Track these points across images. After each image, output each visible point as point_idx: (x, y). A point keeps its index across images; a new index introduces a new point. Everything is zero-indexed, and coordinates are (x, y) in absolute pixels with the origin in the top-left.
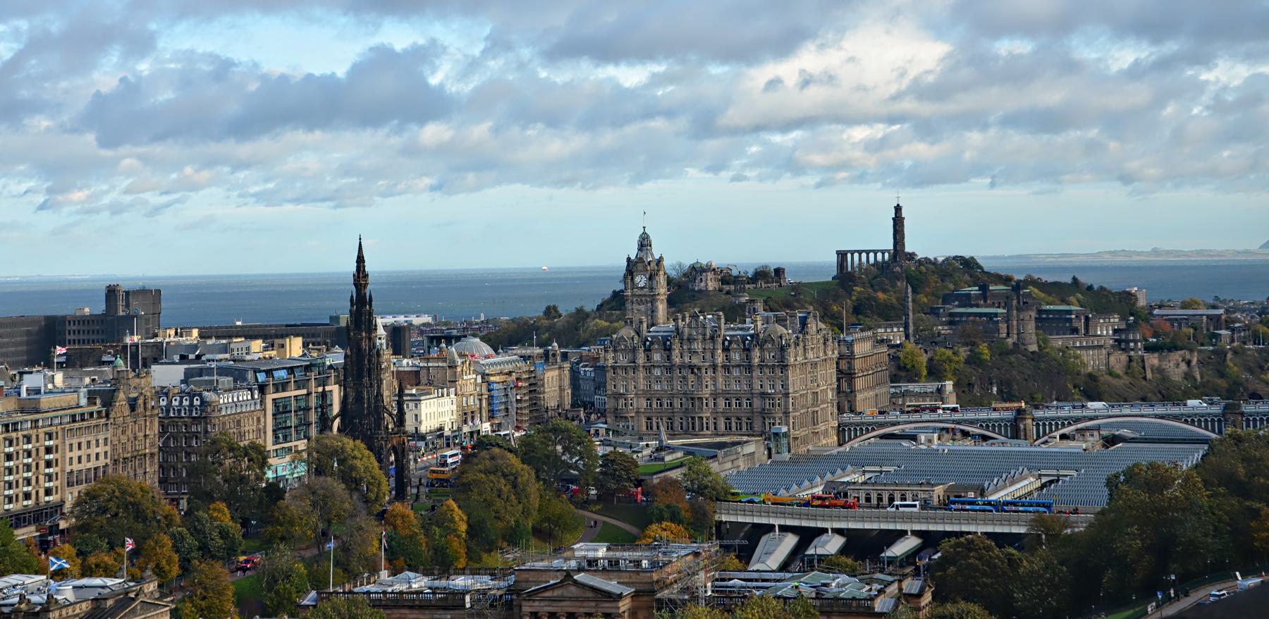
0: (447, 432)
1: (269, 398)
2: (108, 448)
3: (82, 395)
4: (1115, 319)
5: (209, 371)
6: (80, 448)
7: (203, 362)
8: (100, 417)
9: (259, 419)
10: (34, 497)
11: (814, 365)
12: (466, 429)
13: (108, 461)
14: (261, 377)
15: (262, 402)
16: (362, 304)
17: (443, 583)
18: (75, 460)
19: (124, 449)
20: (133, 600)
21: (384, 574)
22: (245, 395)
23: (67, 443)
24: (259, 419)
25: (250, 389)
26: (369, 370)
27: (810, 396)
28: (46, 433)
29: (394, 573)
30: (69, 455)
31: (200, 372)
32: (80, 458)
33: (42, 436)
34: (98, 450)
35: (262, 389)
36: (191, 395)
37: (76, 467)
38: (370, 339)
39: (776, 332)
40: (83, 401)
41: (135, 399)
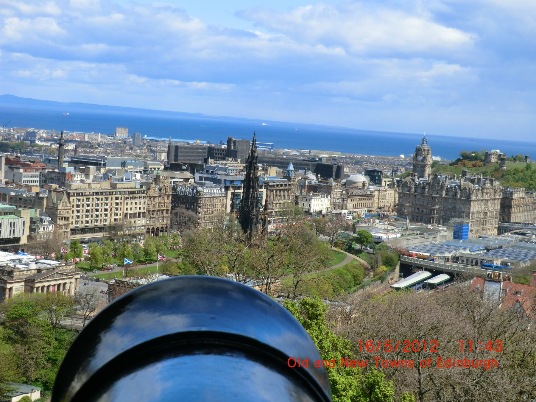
0: (324, 212)
1: (230, 192)
2: (145, 206)
3: (137, 184)
7: (214, 174)
9: (223, 200)
11: (487, 200)
12: (334, 212)
13: (145, 211)
15: (226, 193)
23: (126, 202)
24: (223, 200)
26: (253, 187)
27: (482, 214)
30: (126, 207)
34: (140, 206)
35: (227, 188)
38: (254, 174)
39: (468, 186)
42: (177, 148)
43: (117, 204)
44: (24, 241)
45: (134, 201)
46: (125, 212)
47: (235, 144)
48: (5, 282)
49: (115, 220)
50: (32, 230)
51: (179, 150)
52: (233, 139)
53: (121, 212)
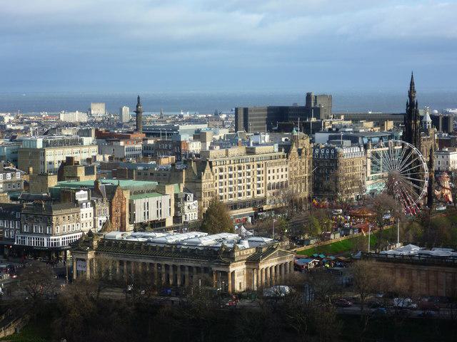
2: (287, 173)
4: (325, 183)
5: (339, 137)
6: (274, 172)
8: (284, 157)
10: (252, 193)
14: (365, 141)
15: (366, 153)
16: (412, 105)
17: (428, 251)
18: (271, 178)
19: (295, 174)
20: (275, 249)
21: (399, 245)
22: (356, 149)
23: (268, 170)
25: (359, 147)
28: (220, 168)
29: (405, 244)
30: (268, 175)
31: (336, 137)
32: (274, 177)
33: (255, 166)
34: (282, 173)
35: (366, 147)
36: (330, 149)
37: (272, 181)
40: (276, 150)
41: (301, 150)
42: (246, 110)
43: (259, 173)
44: (169, 223)
45: (276, 168)
46: (268, 182)
47: (316, 100)
48: (227, 265)
49: (258, 192)
50: (177, 209)
51: (249, 113)
52: (313, 95)
53: (263, 182)
